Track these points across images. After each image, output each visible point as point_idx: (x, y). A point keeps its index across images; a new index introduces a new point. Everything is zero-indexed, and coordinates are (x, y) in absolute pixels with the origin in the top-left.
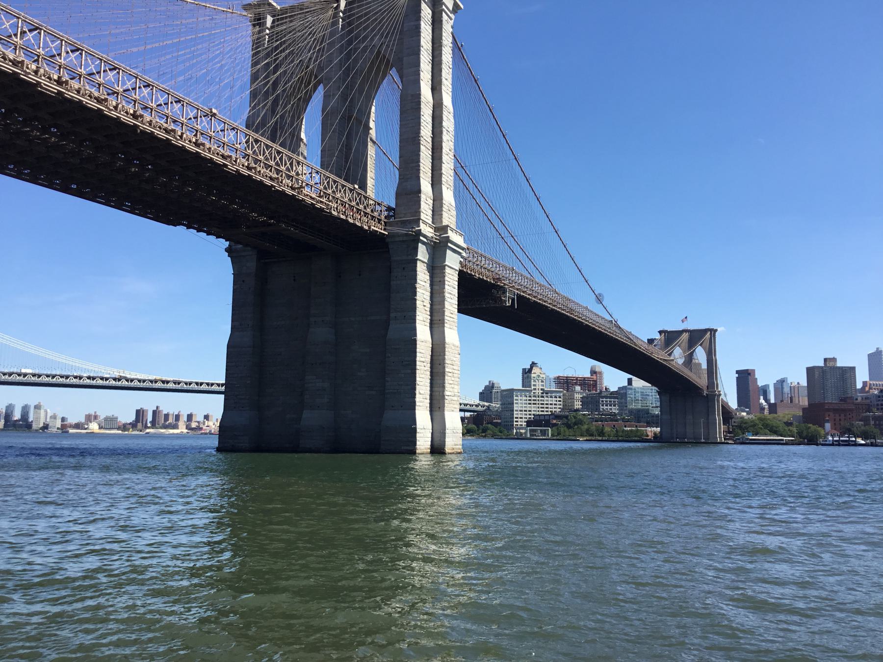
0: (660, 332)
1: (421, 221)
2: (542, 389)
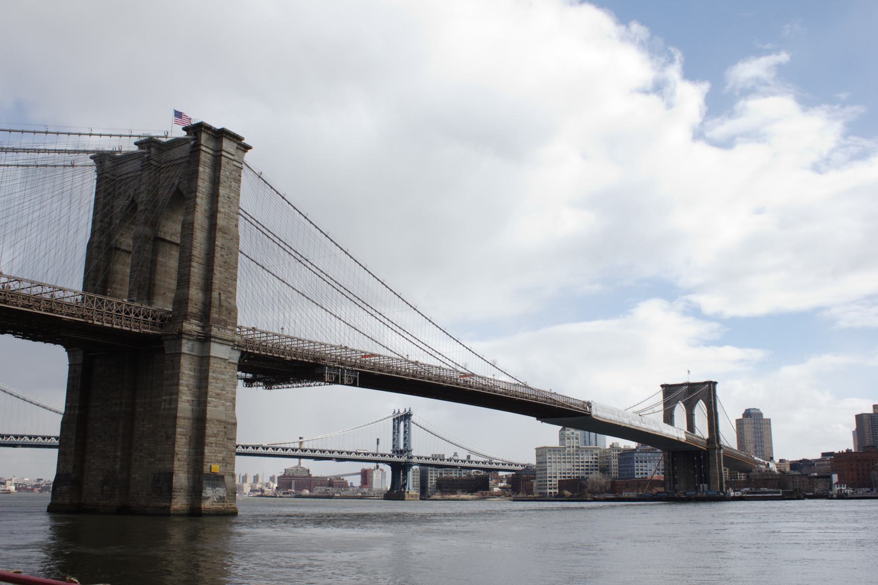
0: (662, 386)
1: (184, 323)
2: (576, 447)
